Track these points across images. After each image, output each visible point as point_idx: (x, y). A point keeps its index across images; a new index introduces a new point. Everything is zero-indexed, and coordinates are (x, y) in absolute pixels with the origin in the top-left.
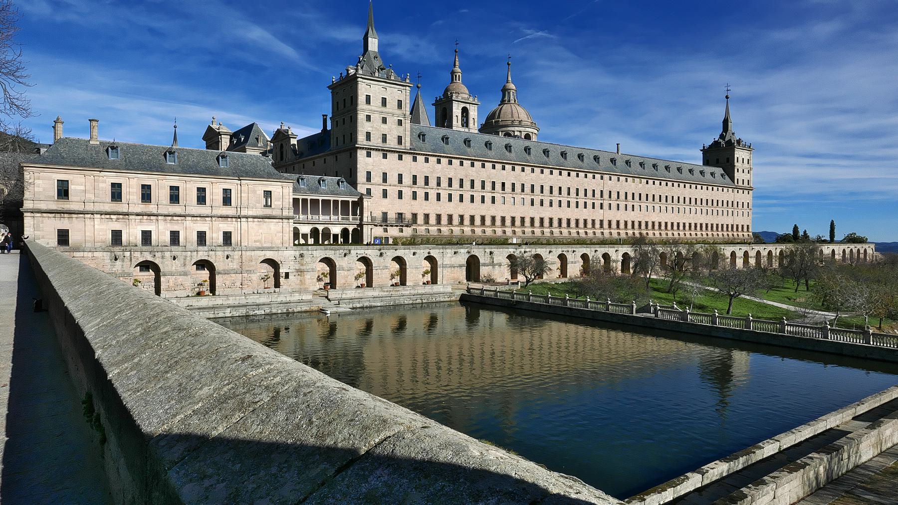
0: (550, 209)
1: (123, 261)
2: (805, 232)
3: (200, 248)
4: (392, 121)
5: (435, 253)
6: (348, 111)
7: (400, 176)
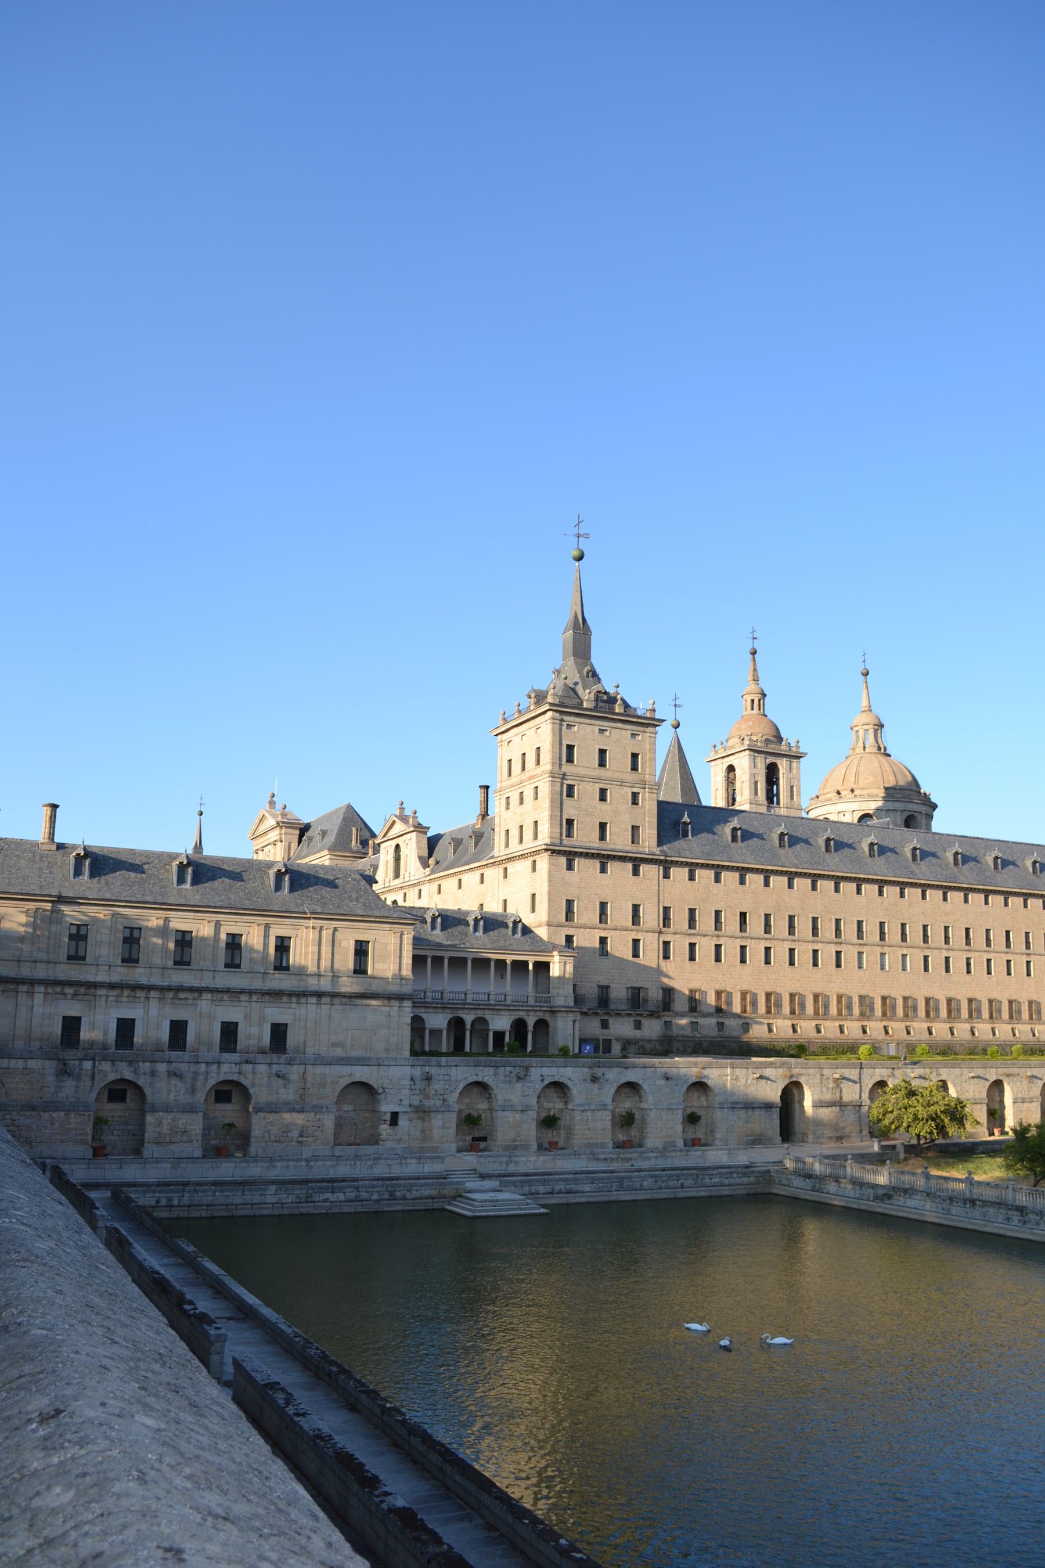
0: (968, 977)
1: (78, 1078)
3: (226, 1056)
4: (620, 796)
6: (531, 777)
7: (636, 908)
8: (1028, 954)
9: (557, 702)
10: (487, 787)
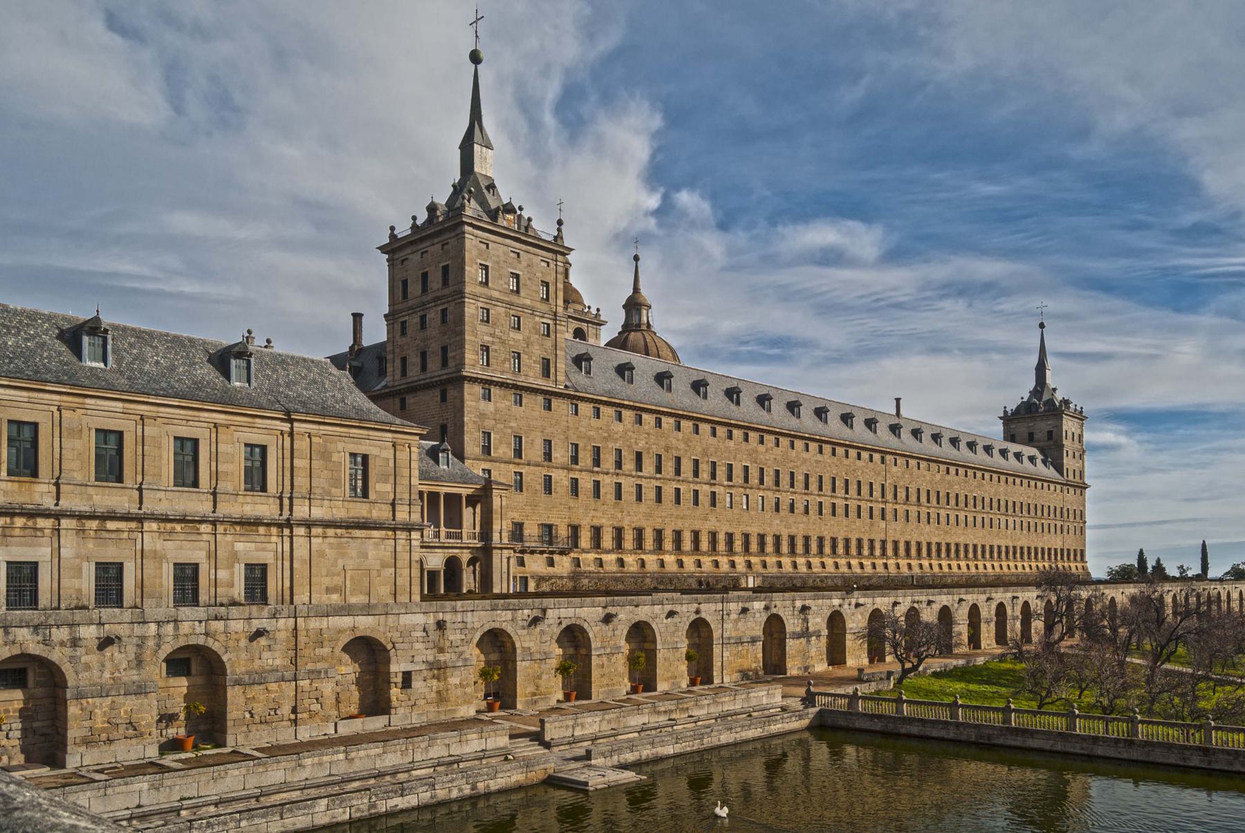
2: (1158, 561)
3: (186, 612)
5: (709, 610)
8: (846, 499)
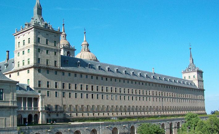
9: (35, 25)
10: (8, 51)
